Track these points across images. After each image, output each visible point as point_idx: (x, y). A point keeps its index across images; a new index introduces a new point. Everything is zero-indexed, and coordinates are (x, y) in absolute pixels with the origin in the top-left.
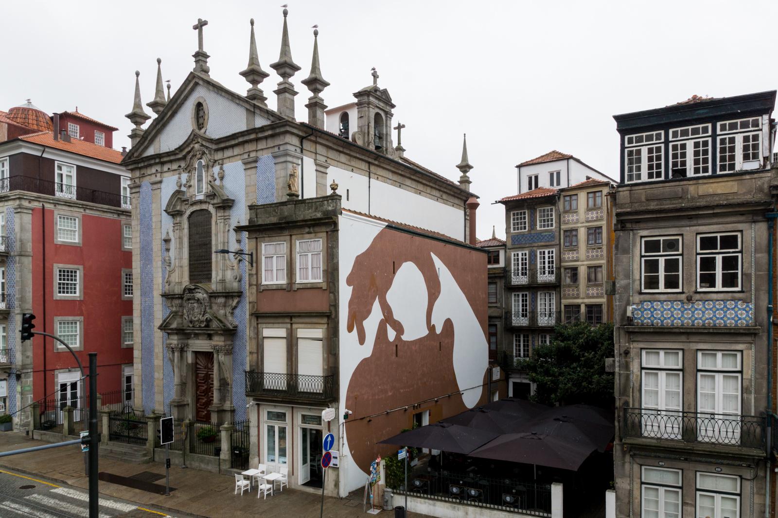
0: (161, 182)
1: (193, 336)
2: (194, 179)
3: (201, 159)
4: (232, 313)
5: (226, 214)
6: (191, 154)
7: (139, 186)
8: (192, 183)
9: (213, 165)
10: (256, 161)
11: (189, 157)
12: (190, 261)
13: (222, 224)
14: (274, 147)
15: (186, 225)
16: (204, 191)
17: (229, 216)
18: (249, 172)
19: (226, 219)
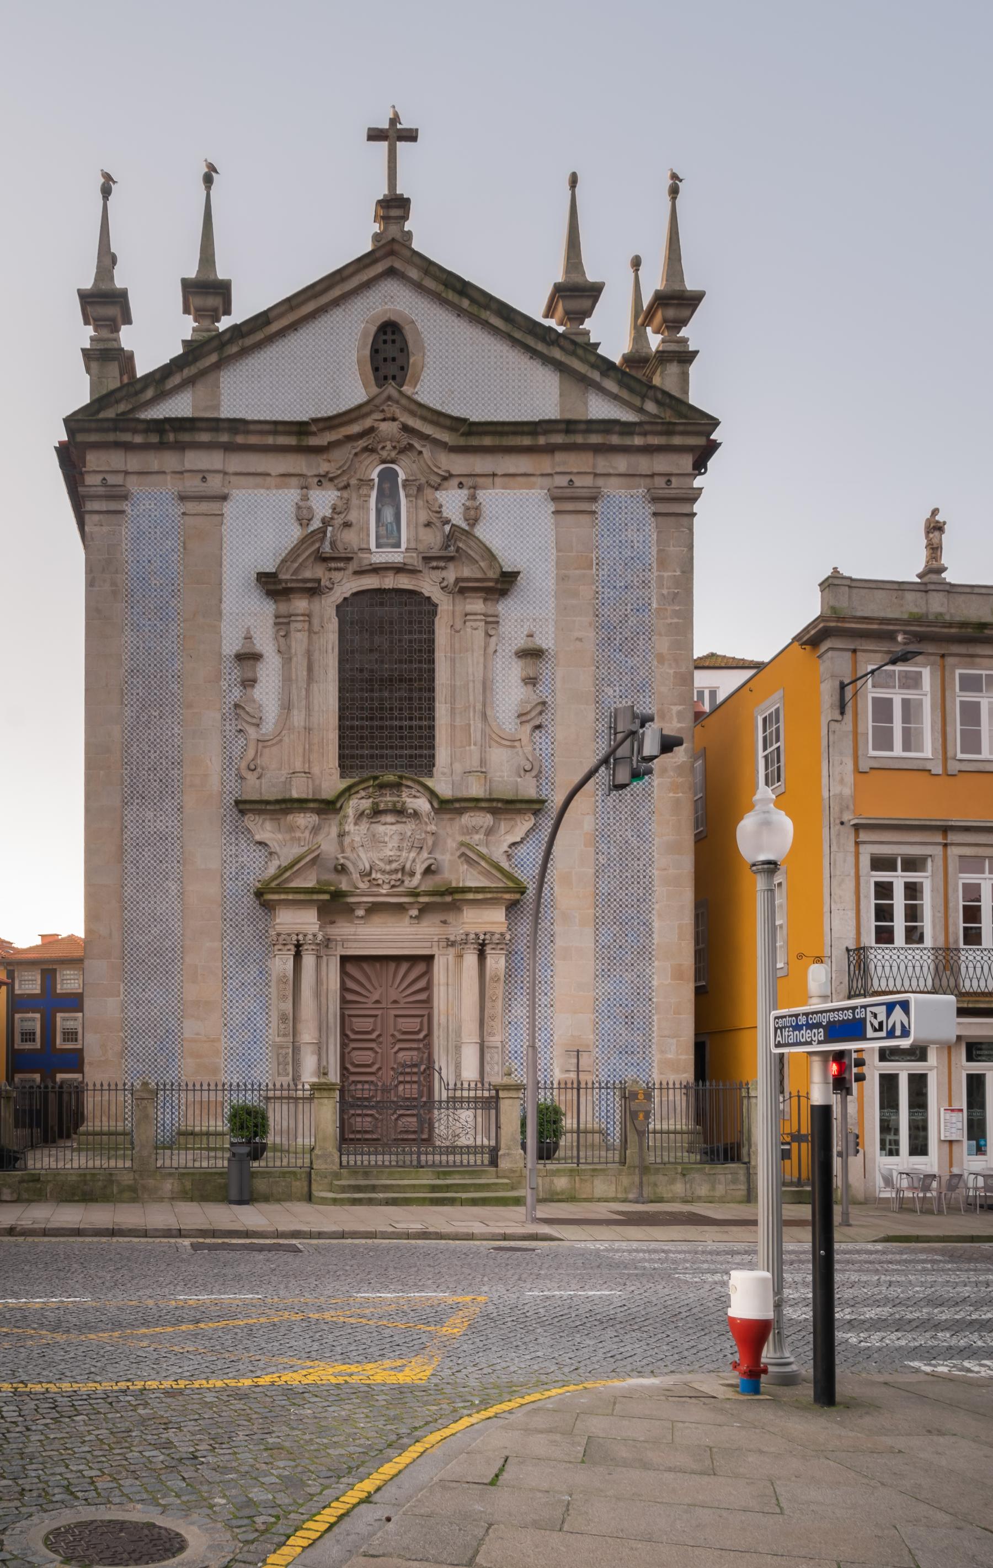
0: (224, 498)
1: (360, 912)
2: (364, 507)
3: (393, 462)
4: (509, 857)
5: (490, 612)
6: (362, 443)
7: (125, 497)
8: (353, 516)
9: (439, 485)
10: (594, 499)
11: (354, 451)
12: (340, 719)
13: (480, 634)
14: (652, 476)
15: (333, 625)
16: (404, 546)
17: (497, 616)
18: (569, 519)
19: (492, 622)
